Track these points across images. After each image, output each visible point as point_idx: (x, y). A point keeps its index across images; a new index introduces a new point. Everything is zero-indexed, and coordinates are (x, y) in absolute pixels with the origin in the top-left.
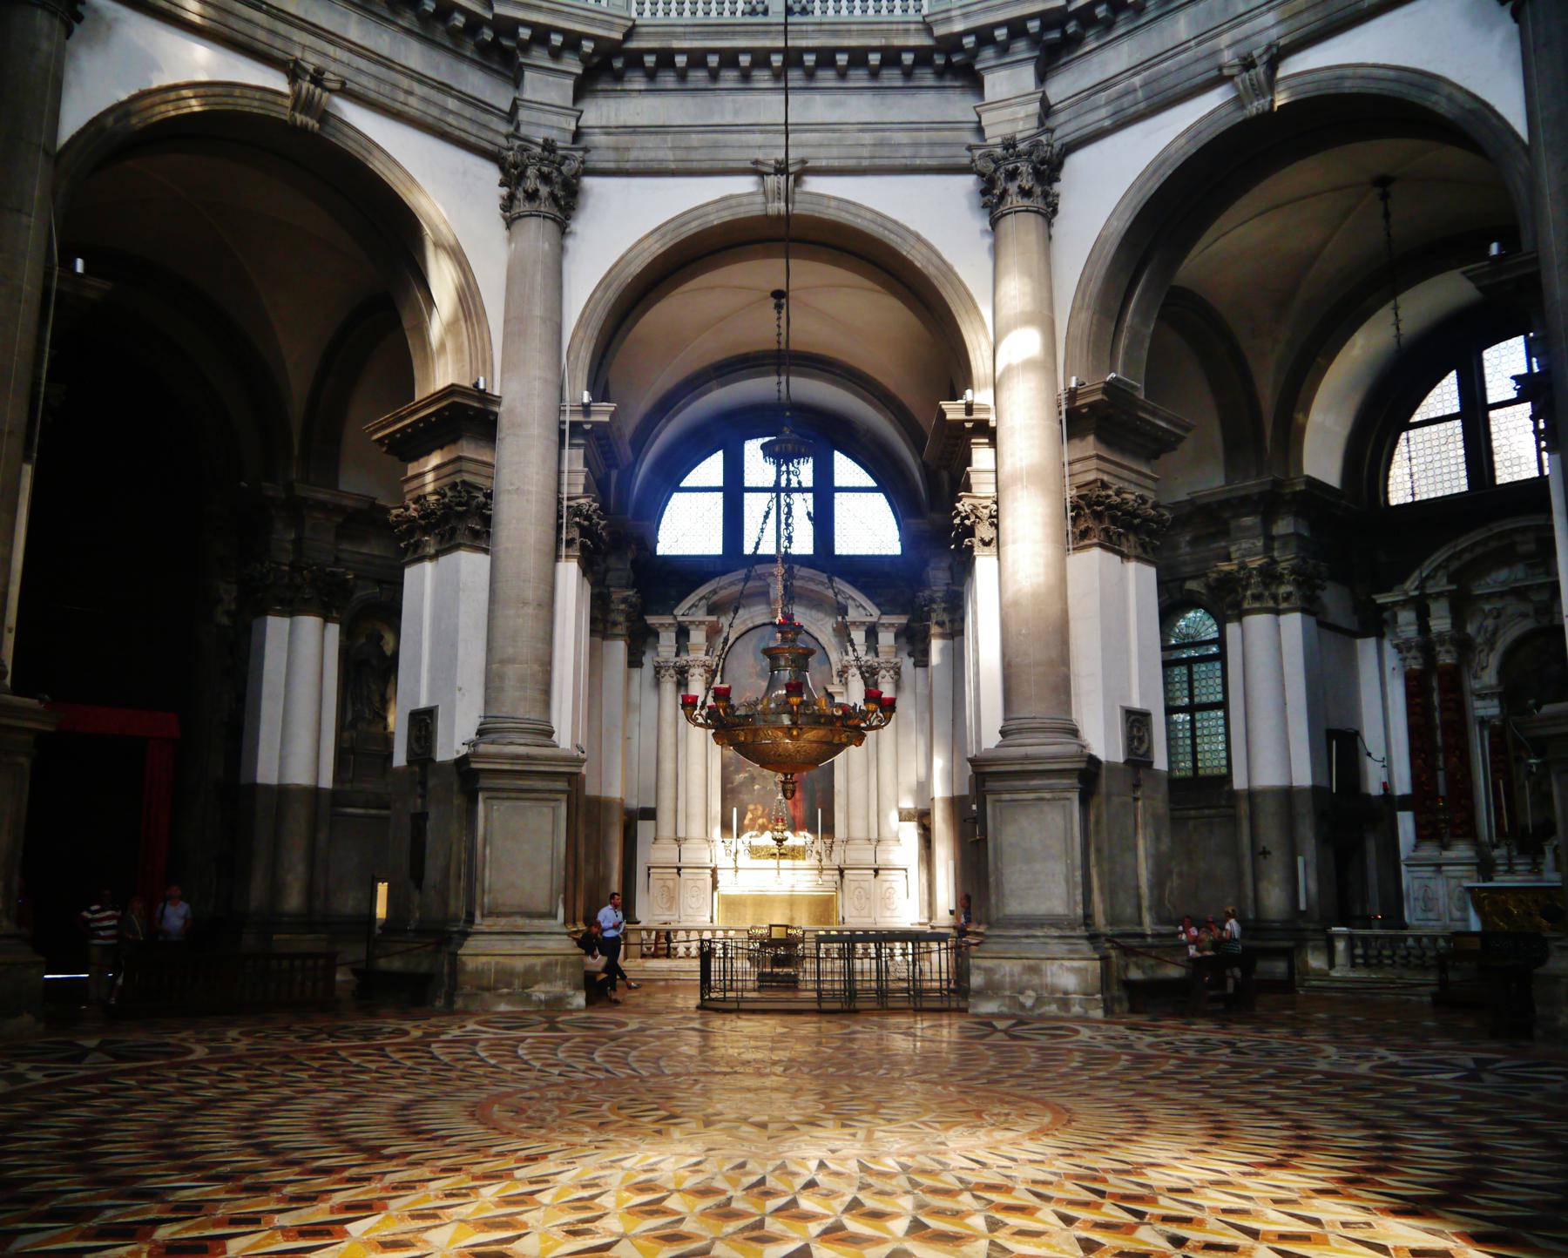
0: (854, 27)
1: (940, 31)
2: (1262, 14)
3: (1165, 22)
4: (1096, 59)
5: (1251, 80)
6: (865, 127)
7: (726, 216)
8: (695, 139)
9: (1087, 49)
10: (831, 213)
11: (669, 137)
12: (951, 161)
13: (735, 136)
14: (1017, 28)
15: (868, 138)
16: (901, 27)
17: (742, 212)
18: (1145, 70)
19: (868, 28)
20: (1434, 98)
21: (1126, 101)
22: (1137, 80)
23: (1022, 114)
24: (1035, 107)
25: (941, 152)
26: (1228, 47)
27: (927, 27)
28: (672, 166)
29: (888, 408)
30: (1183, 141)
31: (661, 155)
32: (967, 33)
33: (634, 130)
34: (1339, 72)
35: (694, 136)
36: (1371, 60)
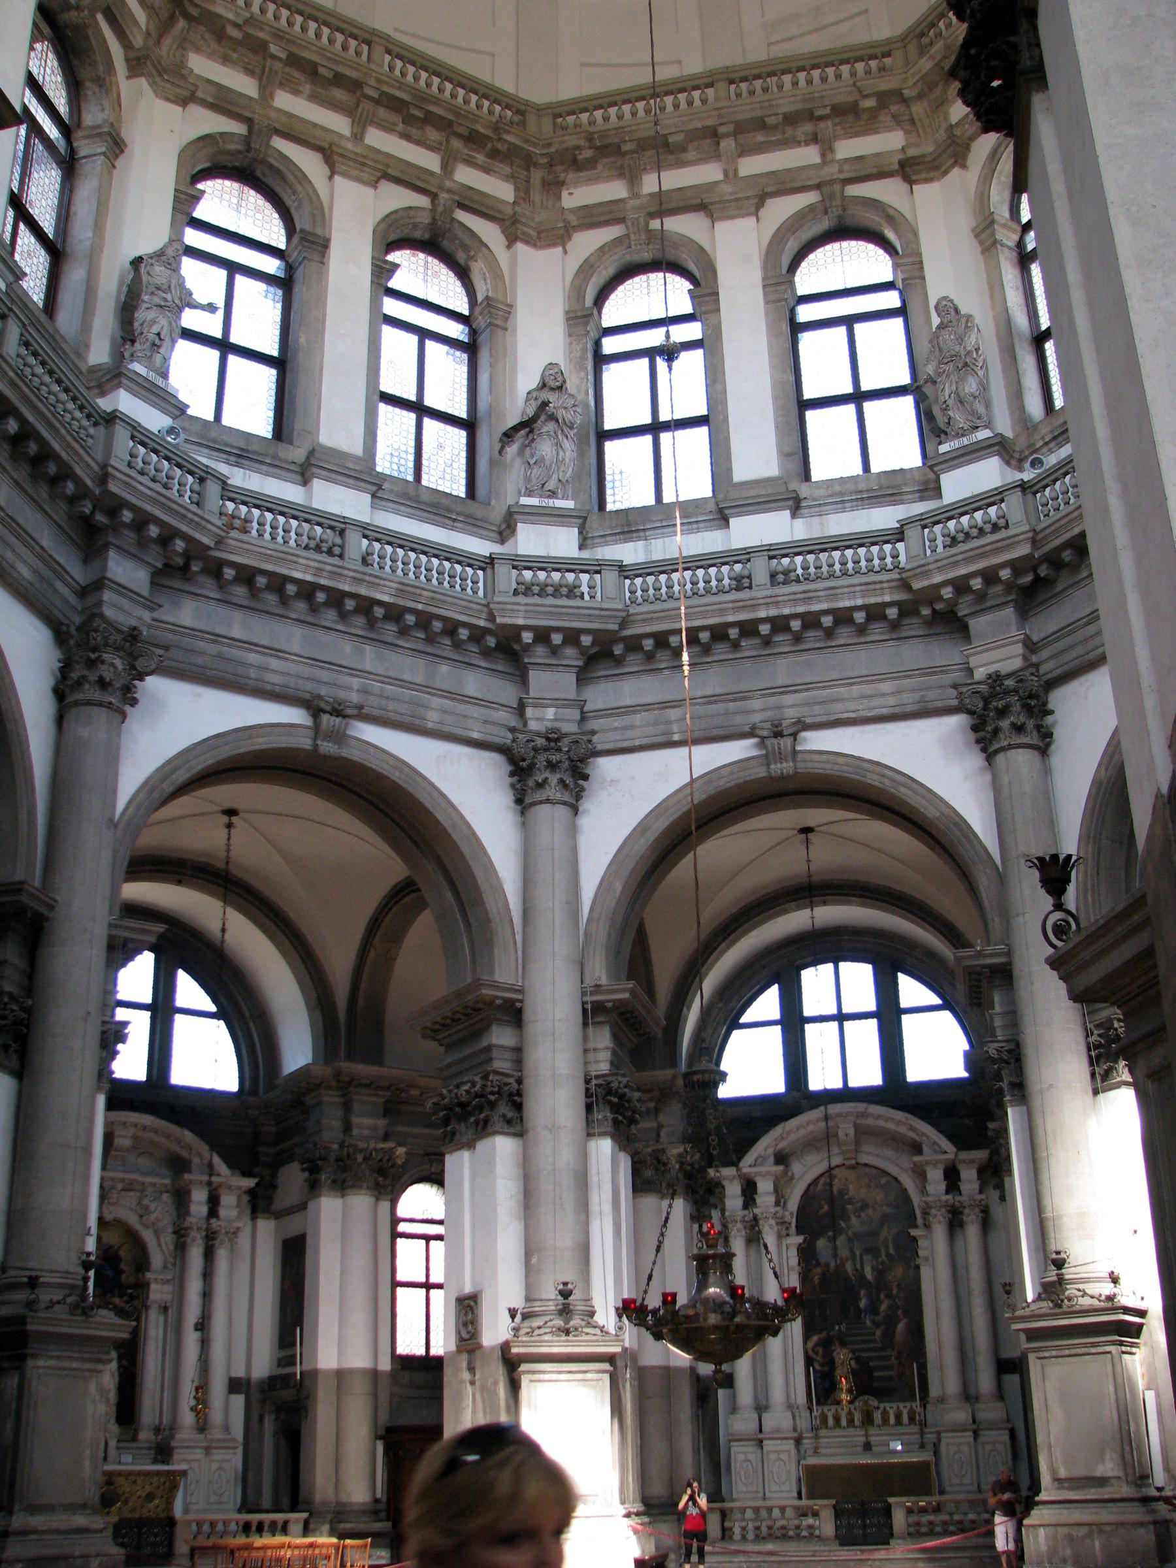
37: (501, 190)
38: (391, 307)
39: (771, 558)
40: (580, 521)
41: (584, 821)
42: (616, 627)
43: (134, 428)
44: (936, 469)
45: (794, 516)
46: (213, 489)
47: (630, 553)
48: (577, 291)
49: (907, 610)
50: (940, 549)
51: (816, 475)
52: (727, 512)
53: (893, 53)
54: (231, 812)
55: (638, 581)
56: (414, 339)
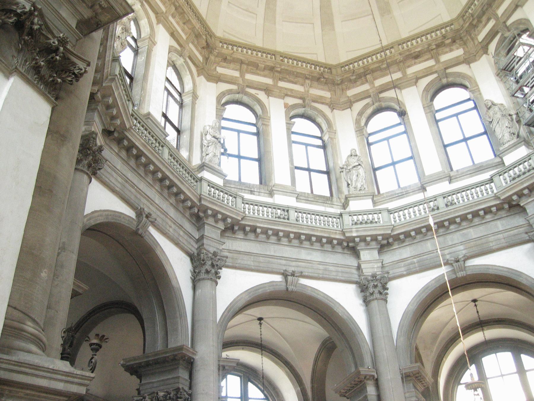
0: (319, 229)
1: (347, 235)
2: (459, 246)
3: (422, 243)
4: (397, 252)
5: (459, 265)
6: (320, 263)
7: (272, 289)
8: (261, 259)
9: (394, 248)
10: (309, 292)
11: (252, 257)
12: (349, 279)
13: (276, 260)
14: (374, 238)
15: (321, 267)
16: (334, 231)
17: (277, 288)
18: (418, 257)
19: (323, 230)
20: (521, 278)
21: (411, 266)
22: (415, 260)
23: (376, 266)
24: (380, 265)
25: (346, 275)
26: (448, 254)
27: (343, 233)
28: (253, 268)
29: (287, 367)
30: (433, 282)
31: (249, 263)
32: (357, 237)
33: (239, 252)
34: (487, 267)
35: (261, 258)
36: (498, 265)
37: (327, 94)
38: (294, 137)
39: (444, 198)
40: (372, 197)
41: (389, 306)
42: (390, 232)
43: (209, 182)
44: (500, 156)
45: (450, 183)
46: (239, 200)
47: (391, 205)
48: (358, 122)
49: (500, 208)
50: (509, 182)
51: (455, 169)
52: (424, 185)
53: (454, 24)
54: (260, 319)
55: (396, 214)
56: (304, 147)
